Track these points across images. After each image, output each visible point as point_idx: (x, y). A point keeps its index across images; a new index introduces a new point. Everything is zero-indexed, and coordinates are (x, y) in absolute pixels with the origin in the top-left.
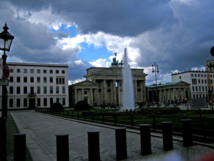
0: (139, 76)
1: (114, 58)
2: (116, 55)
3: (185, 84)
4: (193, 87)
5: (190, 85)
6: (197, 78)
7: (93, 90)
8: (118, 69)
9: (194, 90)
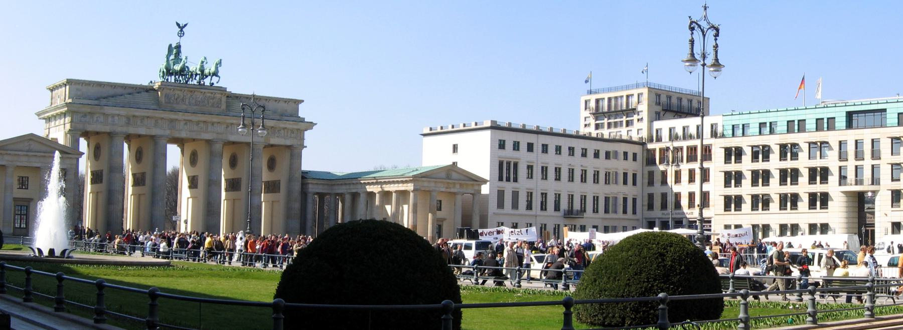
1: (173, 46)
5: (484, 181)
6: (523, 158)
9: (501, 205)
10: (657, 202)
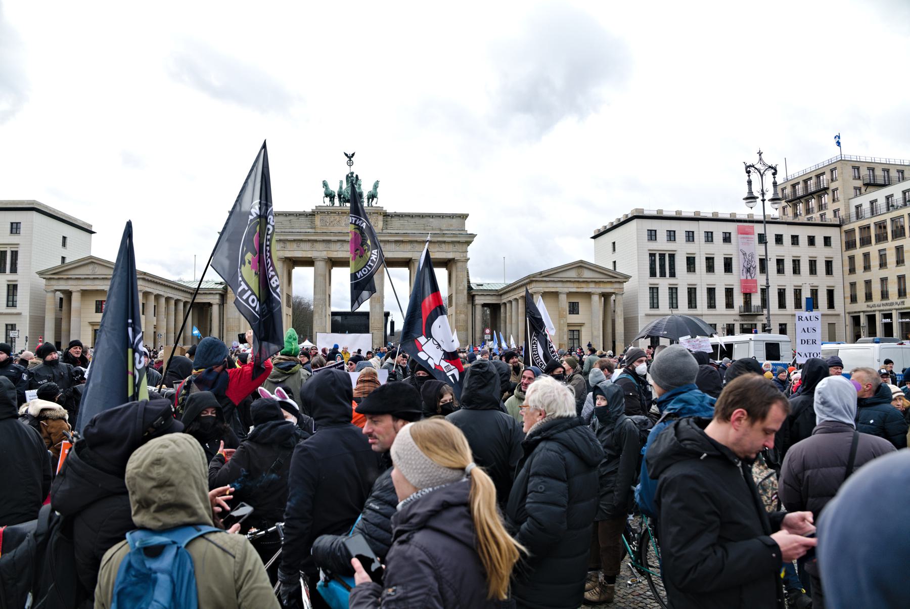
2: (350, 162)
4: (654, 291)
6: (682, 249)
8: (337, 218)
9: (654, 304)
10: (861, 293)
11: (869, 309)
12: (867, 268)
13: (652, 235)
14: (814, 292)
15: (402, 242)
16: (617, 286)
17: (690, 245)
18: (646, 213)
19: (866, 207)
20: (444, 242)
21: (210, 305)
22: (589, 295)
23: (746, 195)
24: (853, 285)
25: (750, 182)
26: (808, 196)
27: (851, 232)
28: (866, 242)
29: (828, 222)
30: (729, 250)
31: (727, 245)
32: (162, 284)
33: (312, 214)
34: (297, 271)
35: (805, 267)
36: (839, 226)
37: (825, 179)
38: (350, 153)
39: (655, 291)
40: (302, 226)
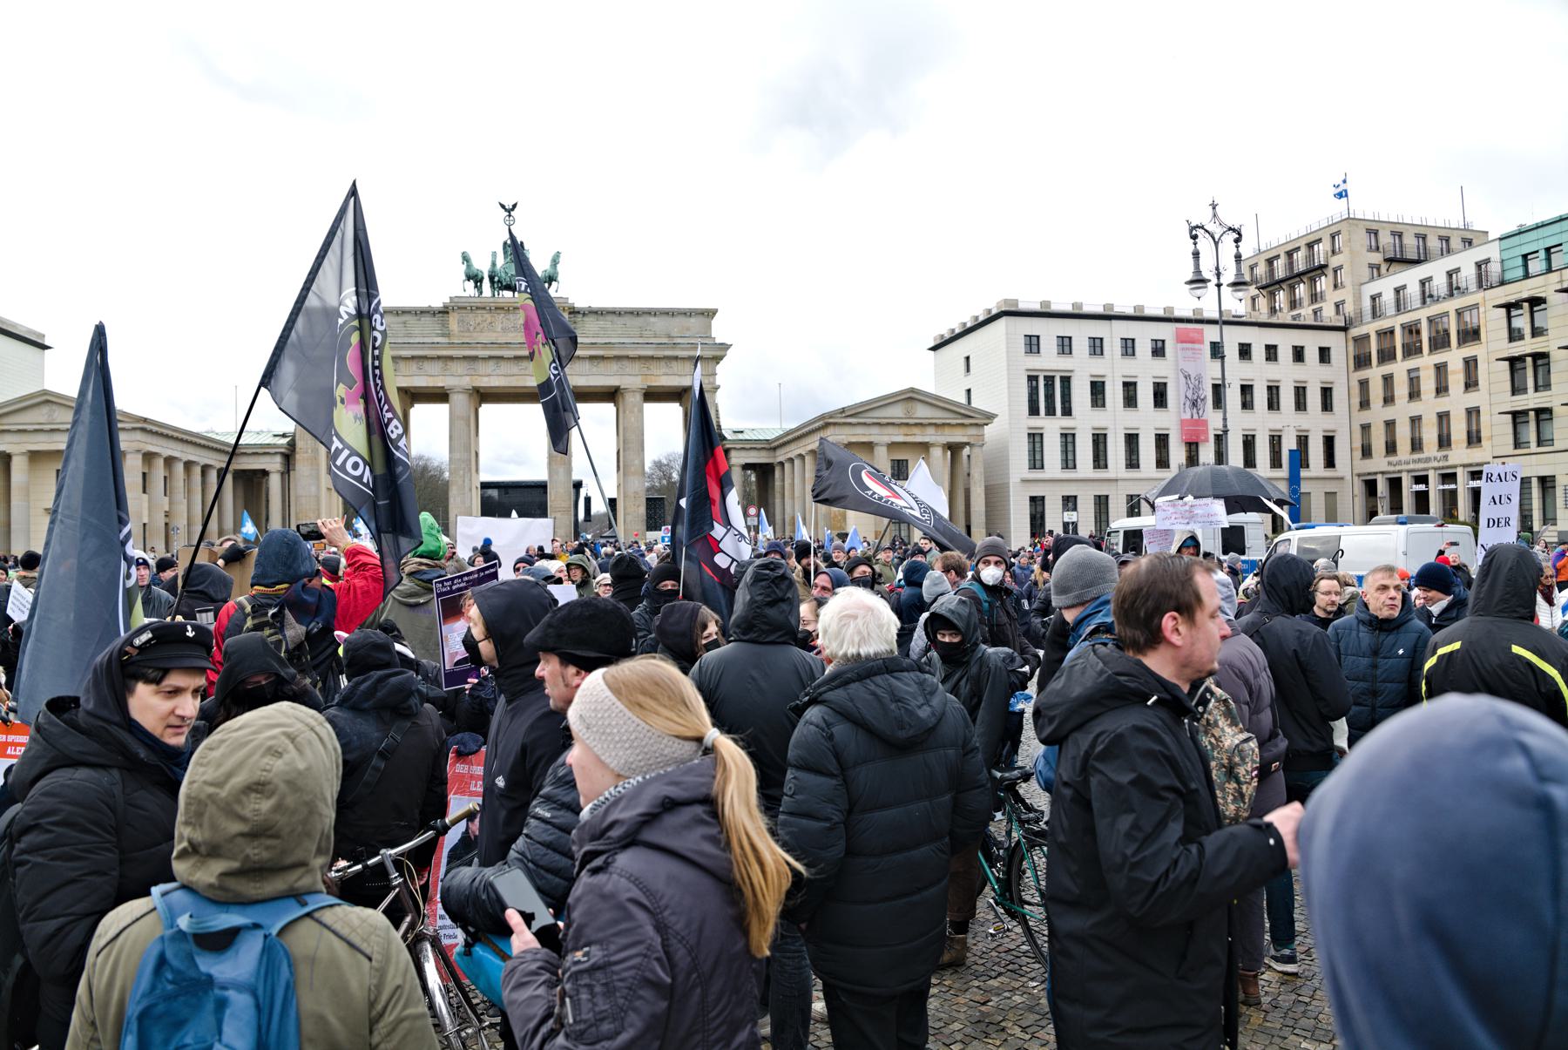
0: (652, 358)
3: (939, 414)
4: (1036, 439)
6: (1083, 369)
7: (149, 457)
8: (488, 316)
9: (1036, 462)
10: (1378, 441)
11: (1391, 468)
12: (1389, 399)
13: (1033, 344)
14: (1303, 441)
15: (603, 358)
16: (973, 431)
17: (1097, 361)
18: (1022, 307)
19: (1388, 298)
20: (676, 358)
21: (265, 473)
22: (925, 447)
23: (1190, 277)
24: (1366, 428)
25: (1196, 255)
26: (1293, 278)
27: (1362, 340)
28: (1387, 356)
29: (1327, 323)
30: (1163, 369)
31: (1158, 362)
32: (177, 439)
33: (444, 311)
34: (419, 412)
35: (1287, 398)
36: (1344, 329)
37: (1322, 250)
38: (509, 205)
39: (1037, 439)
40: (426, 332)
